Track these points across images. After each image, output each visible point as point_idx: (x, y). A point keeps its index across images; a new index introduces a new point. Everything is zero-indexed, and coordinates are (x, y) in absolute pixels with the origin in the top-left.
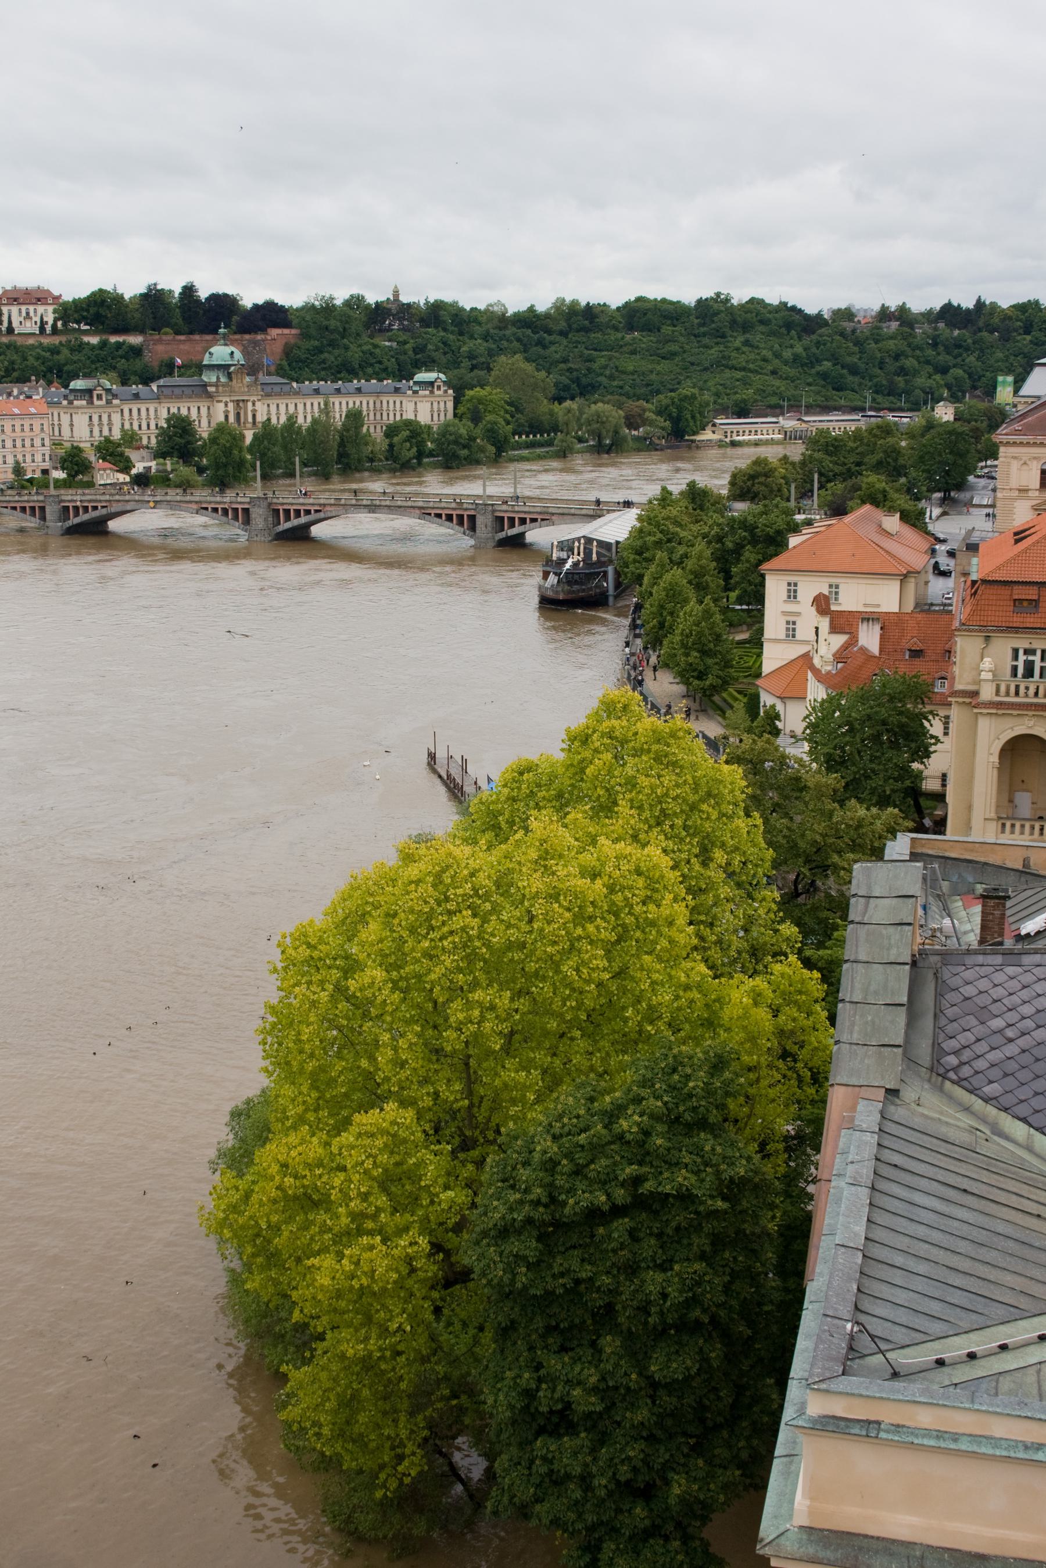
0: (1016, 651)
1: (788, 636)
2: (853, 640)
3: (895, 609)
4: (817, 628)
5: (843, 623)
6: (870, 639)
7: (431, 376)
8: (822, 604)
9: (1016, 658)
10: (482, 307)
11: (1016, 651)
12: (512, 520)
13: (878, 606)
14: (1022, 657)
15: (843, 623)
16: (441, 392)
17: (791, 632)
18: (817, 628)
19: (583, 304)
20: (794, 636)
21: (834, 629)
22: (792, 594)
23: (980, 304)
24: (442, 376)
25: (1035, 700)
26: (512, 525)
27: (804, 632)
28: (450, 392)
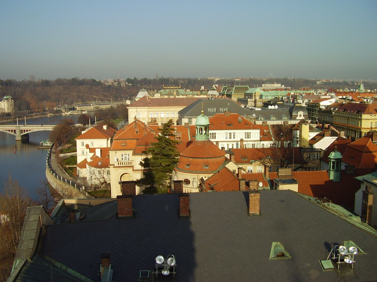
0: (122, 155)
1: (82, 154)
2: (95, 154)
3: (106, 147)
4: (87, 152)
5: (92, 150)
6: (98, 153)
7: (8, 97)
8: (87, 146)
9: (122, 156)
10: (21, 81)
11: (122, 155)
12: (24, 130)
13: (102, 146)
14: (124, 156)
15: (92, 150)
16: (10, 101)
17: (83, 153)
18: (87, 152)
19: (45, 80)
20: (84, 154)
21: (91, 152)
22: (83, 144)
23: (135, 78)
24: (10, 97)
25: (121, 165)
26: (24, 132)
27: (85, 153)
28: (13, 101)
